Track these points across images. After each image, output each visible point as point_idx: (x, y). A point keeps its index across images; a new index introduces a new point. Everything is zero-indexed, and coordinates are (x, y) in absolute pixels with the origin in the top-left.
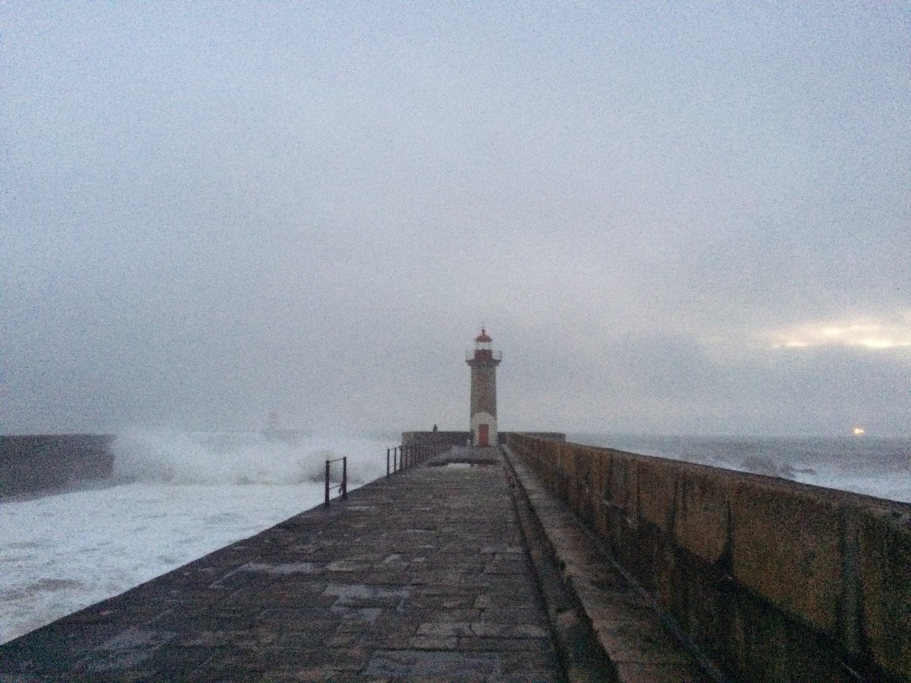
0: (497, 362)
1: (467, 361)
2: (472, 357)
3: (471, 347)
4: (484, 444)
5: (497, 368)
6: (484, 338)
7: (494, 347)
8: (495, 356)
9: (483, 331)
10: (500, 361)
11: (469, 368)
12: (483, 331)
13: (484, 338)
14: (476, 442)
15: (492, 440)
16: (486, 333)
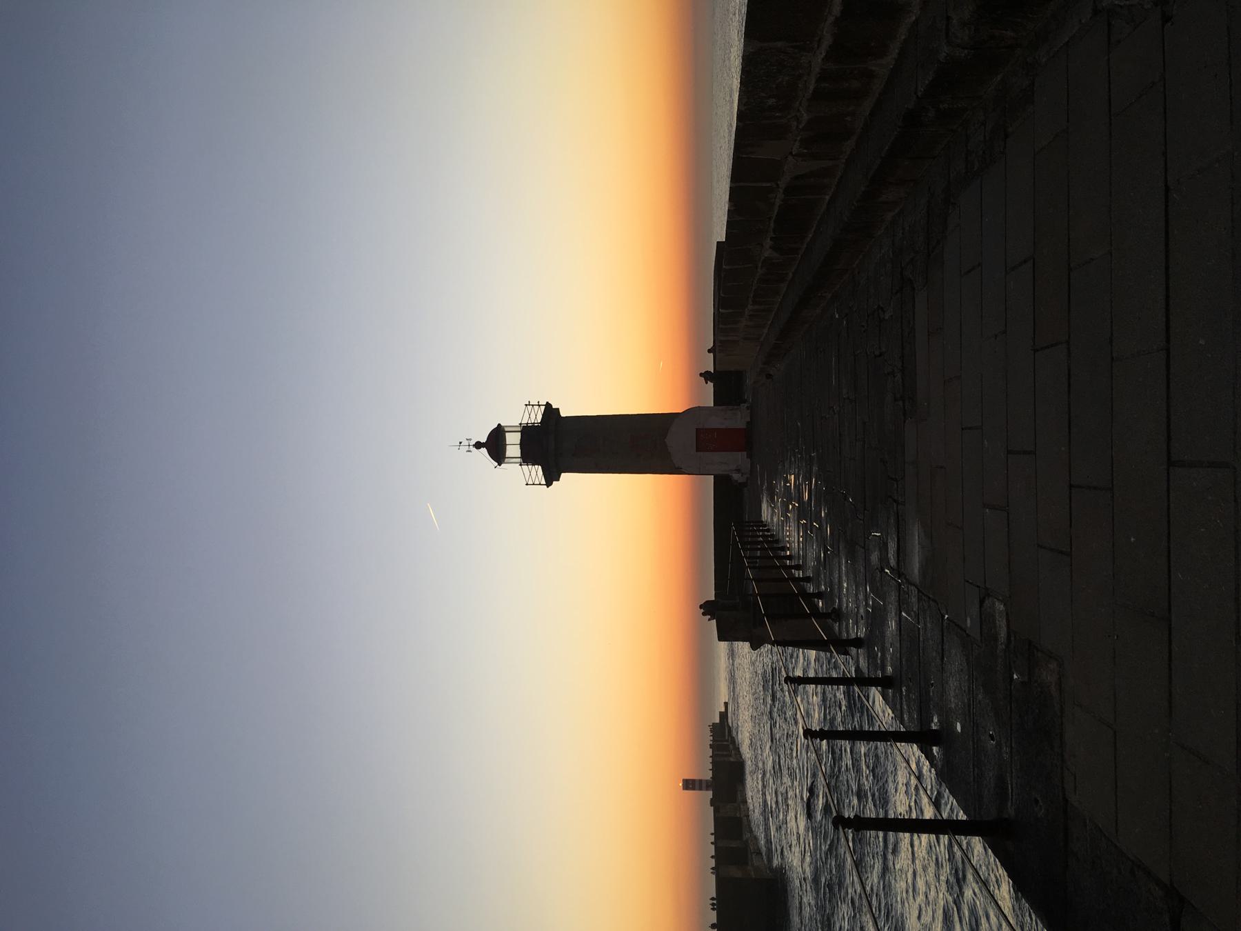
0: (550, 412)
1: (549, 484)
2: (537, 472)
3: (519, 476)
4: (741, 440)
5: (563, 414)
6: (495, 445)
7: (517, 414)
8: (537, 417)
9: (478, 445)
10: (548, 405)
11: (563, 475)
12: (478, 445)
13: (495, 445)
14: (740, 458)
15: (737, 419)
16: (484, 440)
